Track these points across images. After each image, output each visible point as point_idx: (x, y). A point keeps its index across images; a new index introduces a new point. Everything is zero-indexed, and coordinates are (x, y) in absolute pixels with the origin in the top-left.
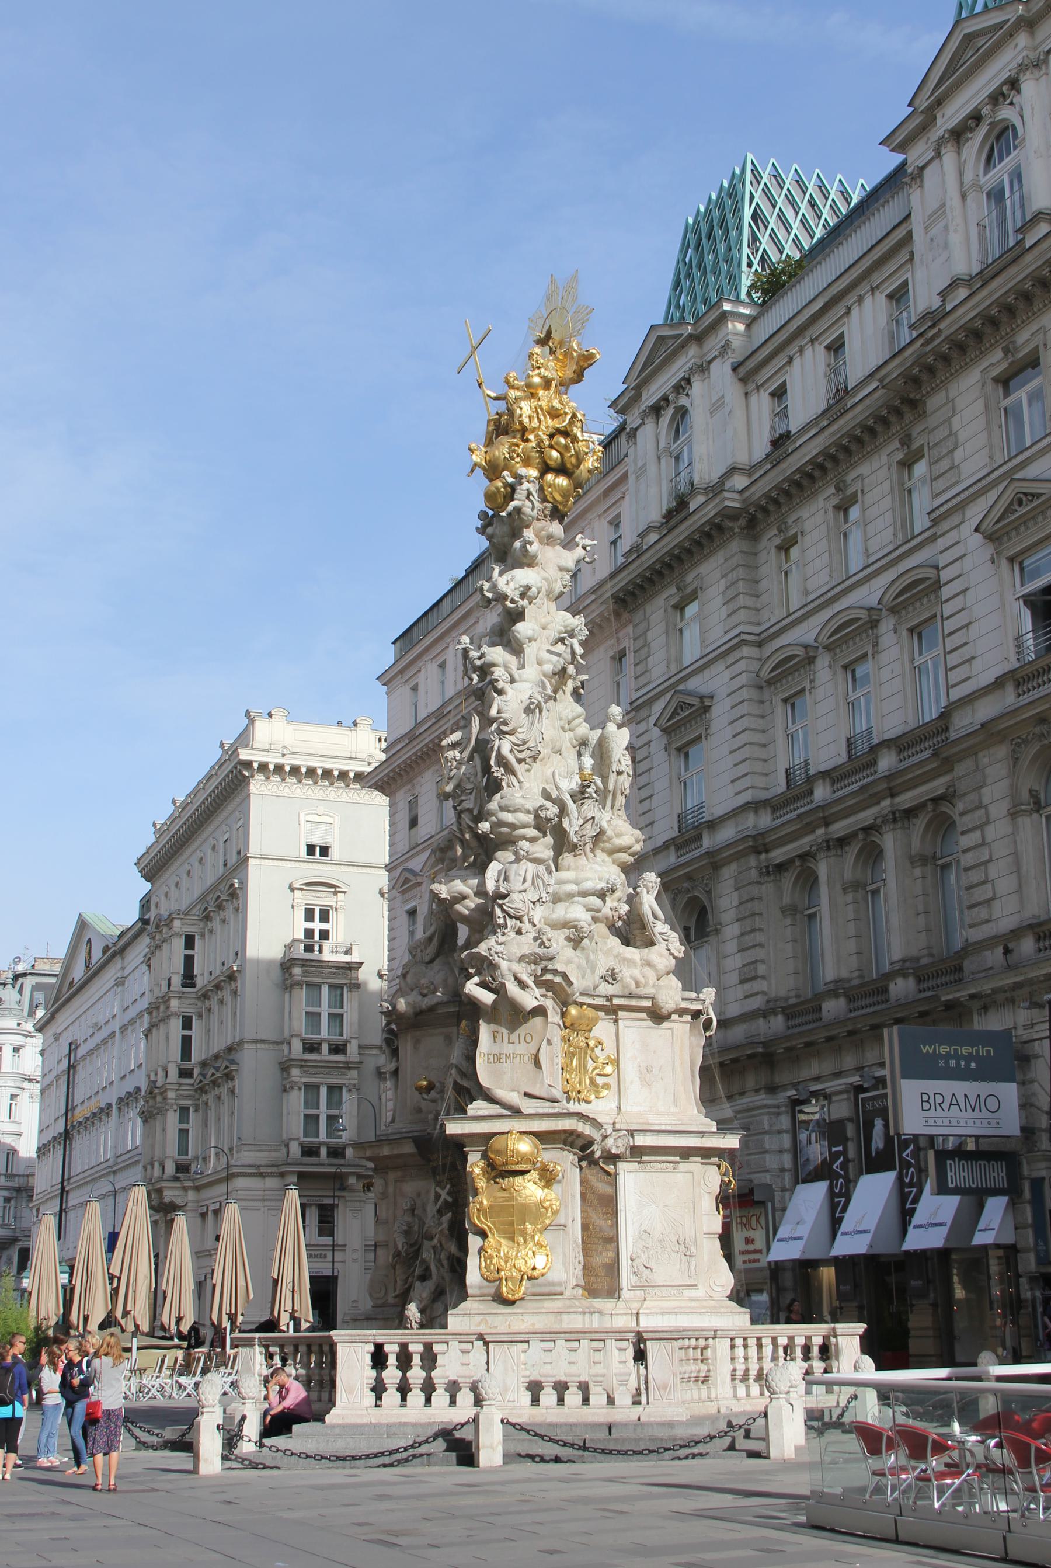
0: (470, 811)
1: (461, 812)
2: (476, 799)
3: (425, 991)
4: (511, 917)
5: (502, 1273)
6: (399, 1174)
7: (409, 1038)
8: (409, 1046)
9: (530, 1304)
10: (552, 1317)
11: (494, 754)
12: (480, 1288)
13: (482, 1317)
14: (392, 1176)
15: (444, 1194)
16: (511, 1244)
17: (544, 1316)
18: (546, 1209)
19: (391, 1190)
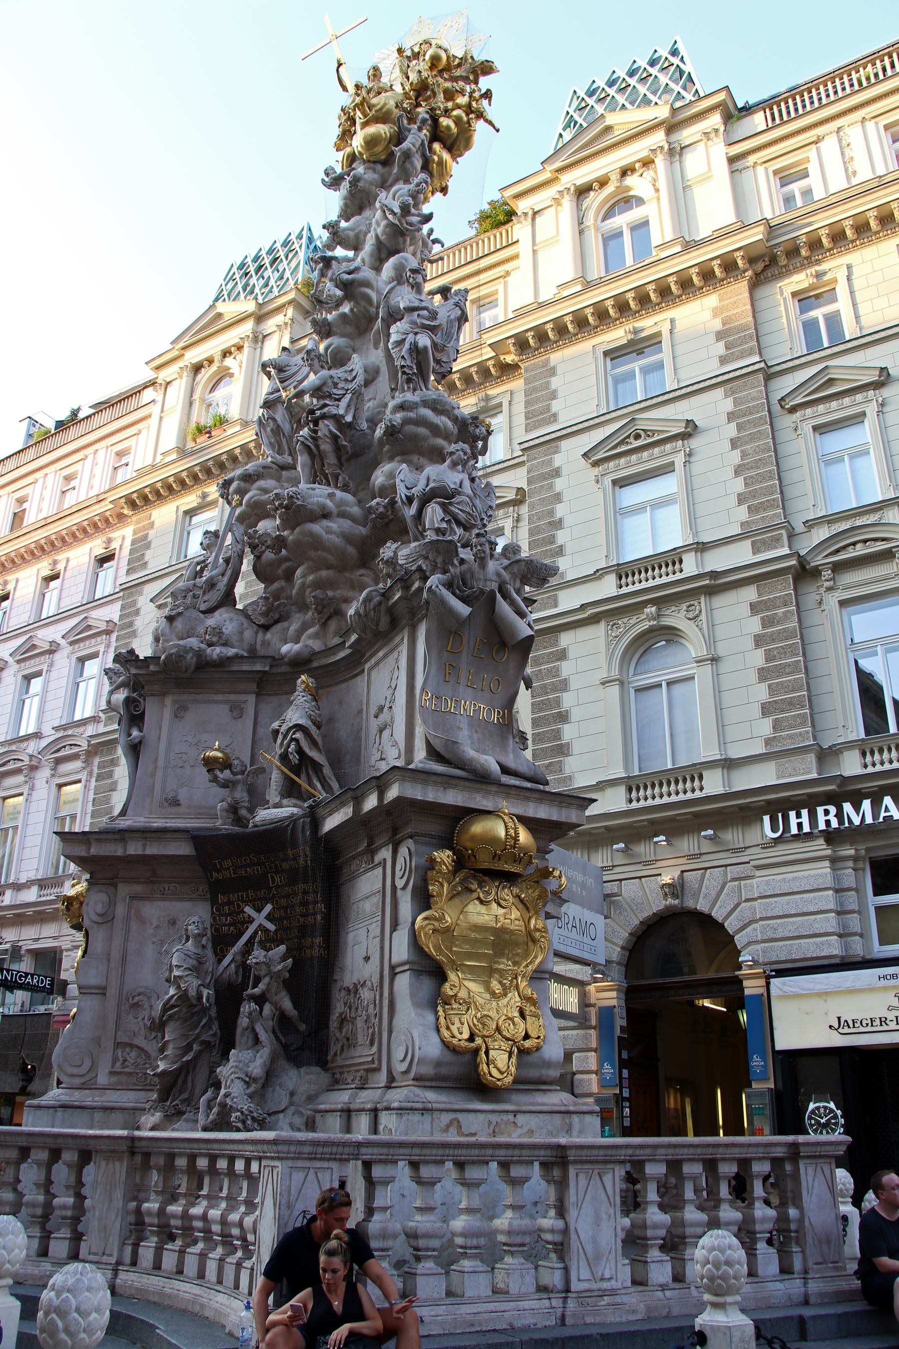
0: (337, 418)
1: (324, 417)
2: (349, 406)
3: (215, 639)
4: (459, 523)
5: (479, 1041)
6: (138, 888)
7: (168, 700)
8: (168, 713)
9: (515, 1097)
10: (557, 1119)
11: (407, 346)
12: (438, 1064)
13: (452, 1116)
14: (124, 890)
15: (260, 918)
16: (488, 996)
17: (547, 1116)
18: (534, 941)
19: (120, 910)
